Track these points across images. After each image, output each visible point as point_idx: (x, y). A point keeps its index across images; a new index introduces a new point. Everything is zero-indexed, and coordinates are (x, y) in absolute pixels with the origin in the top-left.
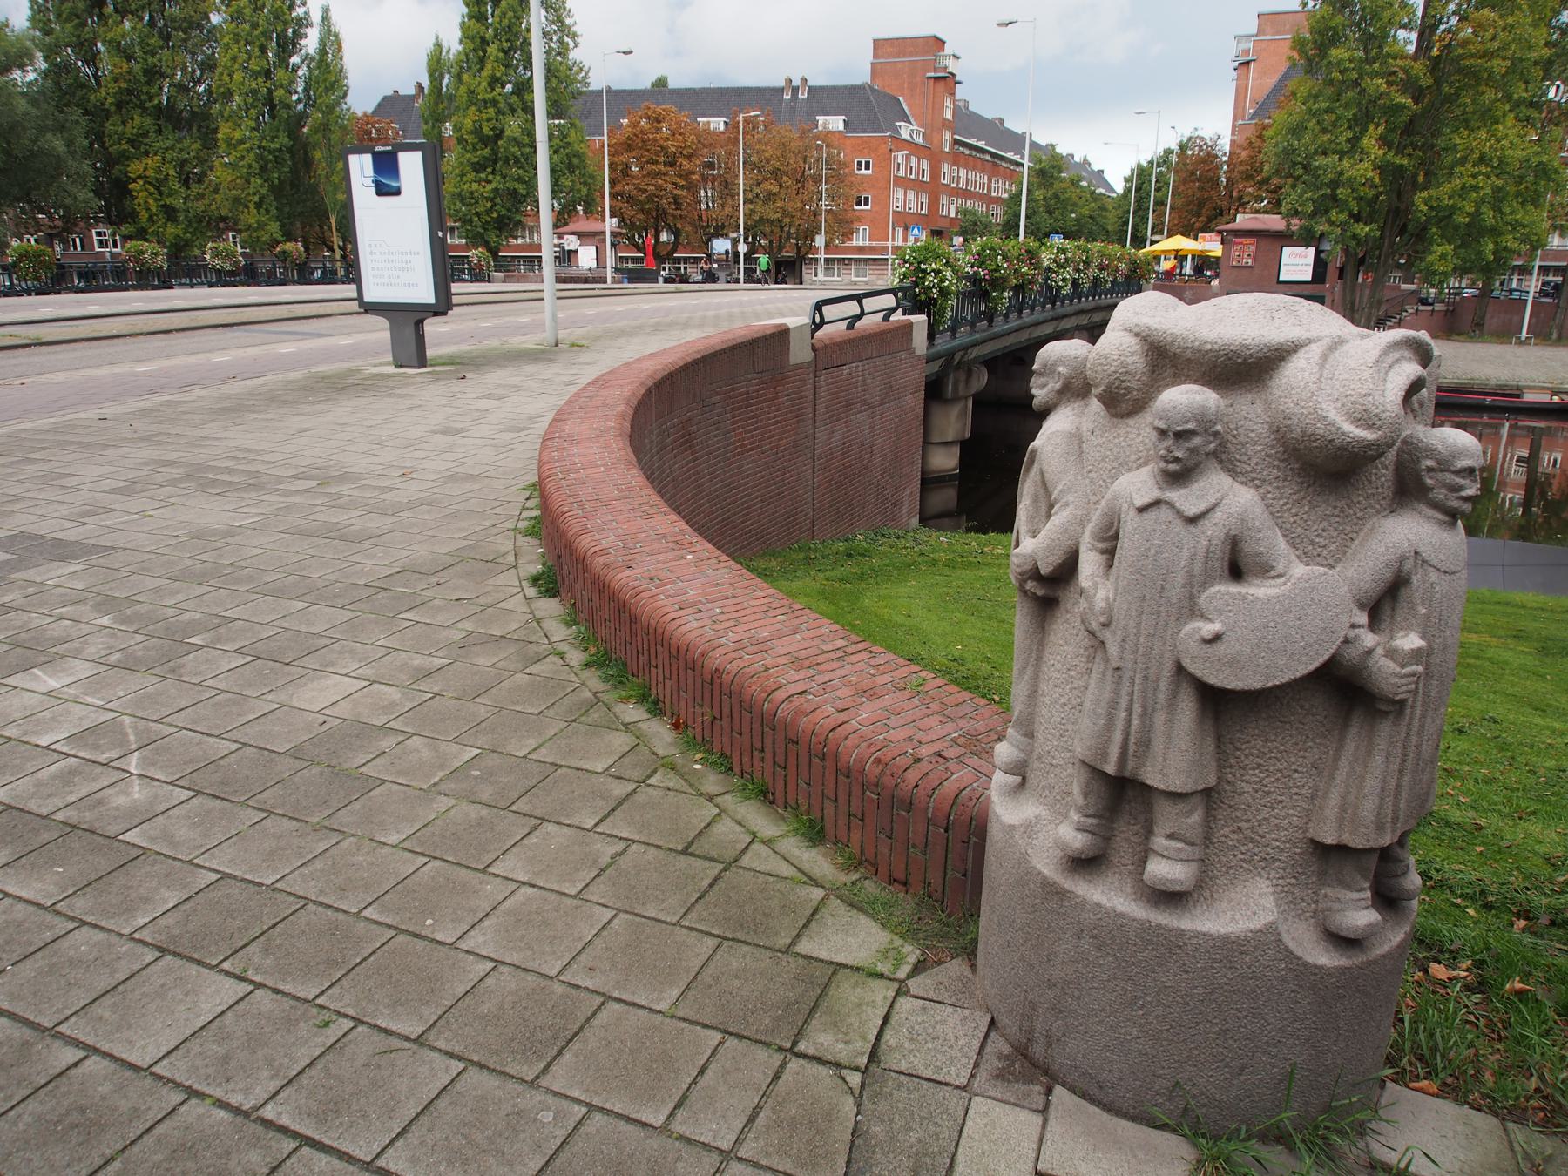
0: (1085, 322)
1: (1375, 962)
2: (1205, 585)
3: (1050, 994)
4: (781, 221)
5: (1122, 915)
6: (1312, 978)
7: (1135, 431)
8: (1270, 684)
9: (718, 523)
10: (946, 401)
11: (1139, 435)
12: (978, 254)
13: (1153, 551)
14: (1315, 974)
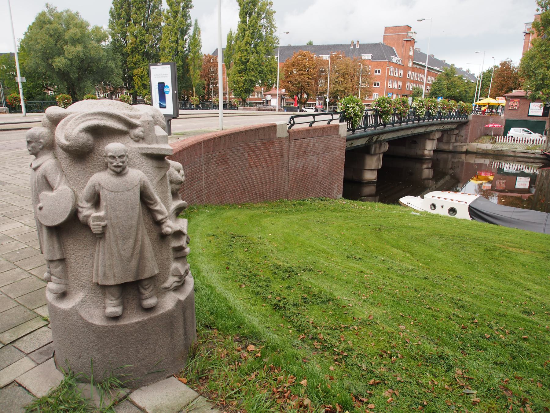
0: (441, 128)
1: (119, 326)
2: (40, 191)
4: (344, 91)
6: (92, 328)
8: (54, 225)
9: (241, 190)
10: (372, 155)
12: (378, 102)
14: (93, 327)
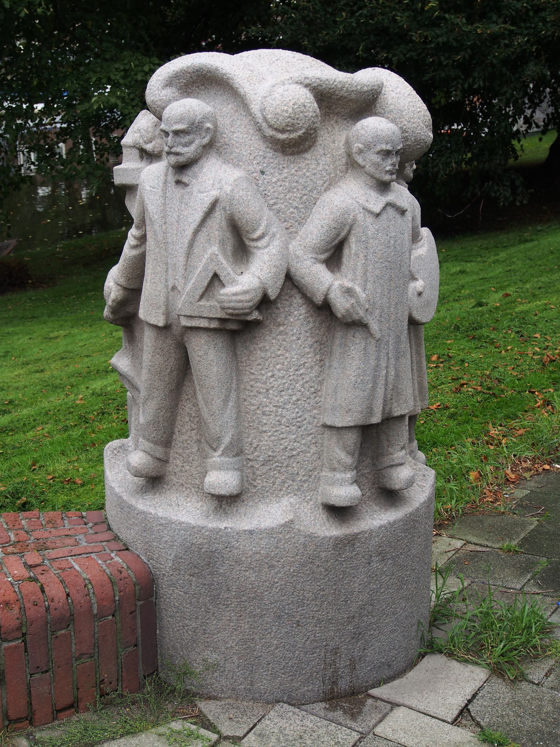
3: (350, 628)
5: (391, 524)
7: (313, 162)
11: (318, 164)
13: (392, 242)
